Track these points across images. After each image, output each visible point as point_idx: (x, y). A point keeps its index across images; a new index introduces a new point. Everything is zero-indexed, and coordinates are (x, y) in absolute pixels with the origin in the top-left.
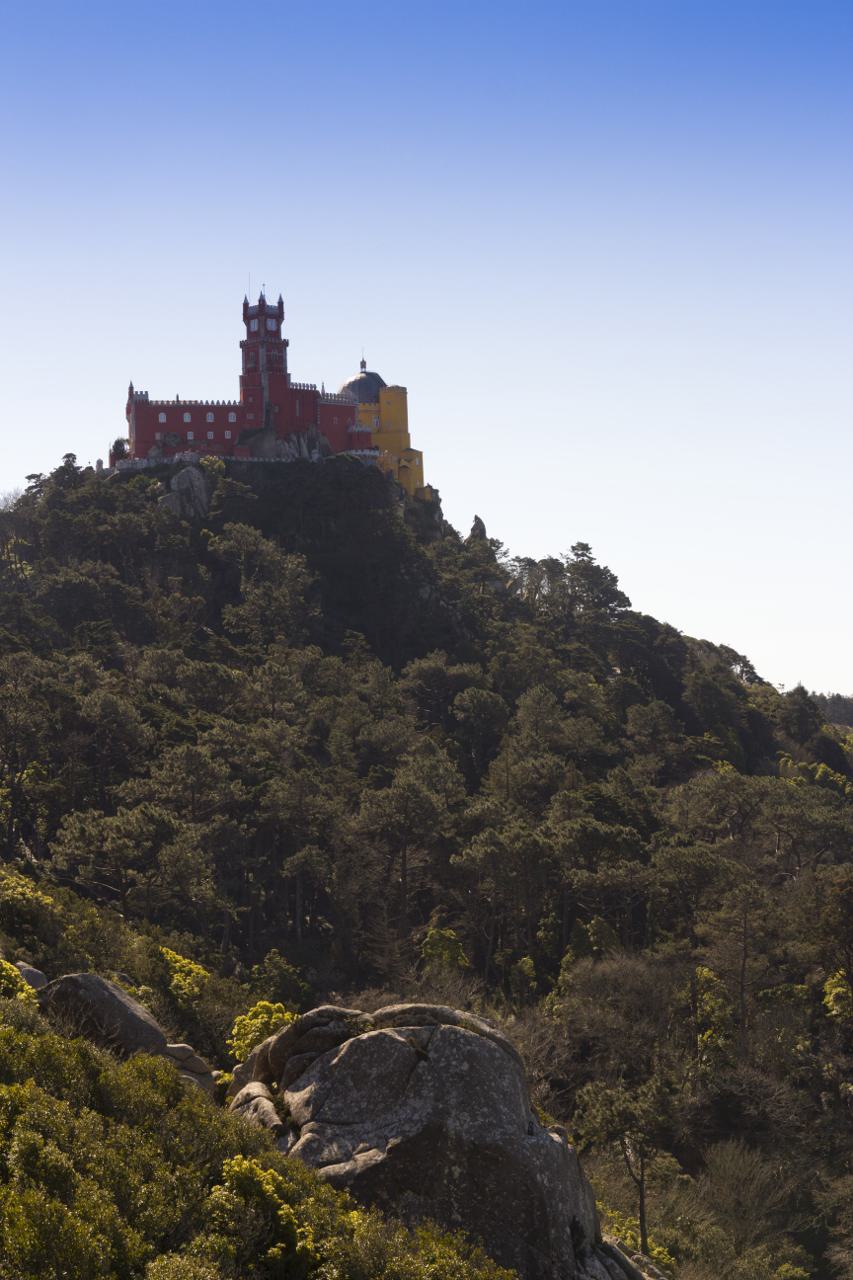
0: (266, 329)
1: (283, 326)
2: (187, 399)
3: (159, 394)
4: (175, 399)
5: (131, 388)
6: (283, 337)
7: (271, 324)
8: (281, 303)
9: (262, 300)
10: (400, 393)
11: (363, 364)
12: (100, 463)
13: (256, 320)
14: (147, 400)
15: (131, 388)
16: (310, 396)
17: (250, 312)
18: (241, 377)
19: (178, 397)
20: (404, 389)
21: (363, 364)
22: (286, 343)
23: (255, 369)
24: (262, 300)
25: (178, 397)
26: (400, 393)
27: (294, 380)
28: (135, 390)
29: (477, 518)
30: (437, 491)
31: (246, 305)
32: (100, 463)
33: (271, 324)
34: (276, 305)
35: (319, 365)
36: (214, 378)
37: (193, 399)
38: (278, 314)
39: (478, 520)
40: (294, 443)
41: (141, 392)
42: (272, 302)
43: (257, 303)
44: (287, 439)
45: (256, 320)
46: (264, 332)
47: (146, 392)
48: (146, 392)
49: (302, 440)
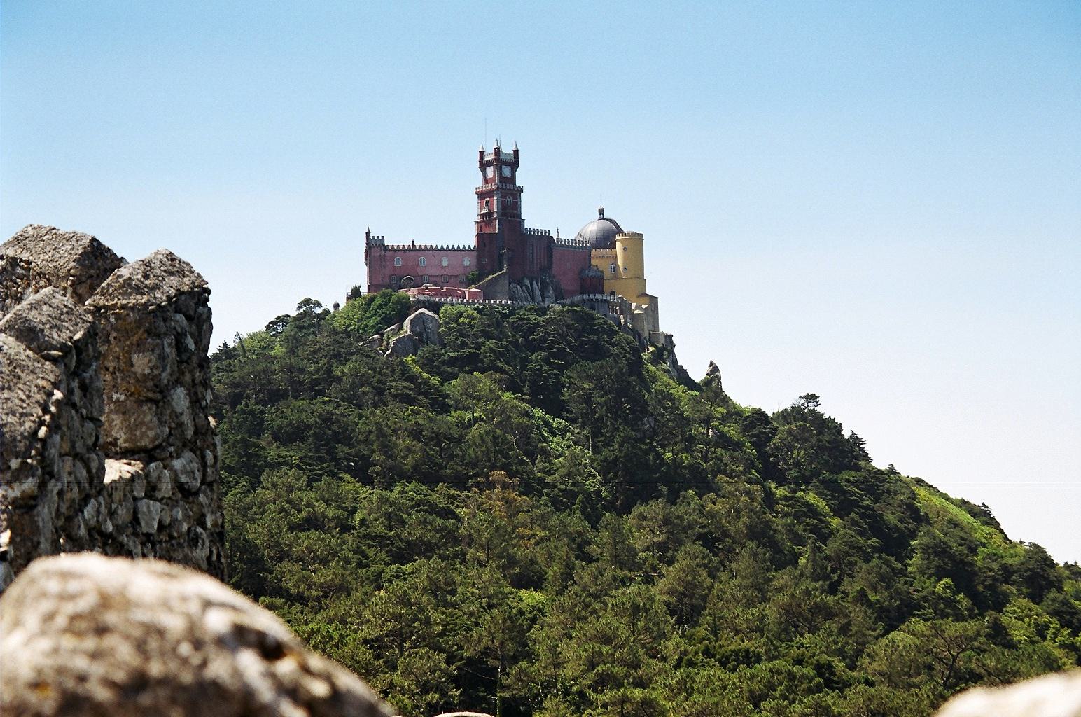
1: (518, 173)
2: (423, 244)
5: (368, 234)
6: (517, 185)
7: (507, 171)
8: (516, 152)
9: (498, 151)
10: (639, 237)
11: (601, 212)
12: (337, 306)
14: (383, 244)
15: (368, 234)
16: (546, 241)
17: (486, 159)
20: (642, 235)
21: (601, 212)
22: (521, 190)
23: (490, 214)
24: (498, 151)
26: (639, 237)
27: (527, 226)
29: (712, 364)
30: (671, 336)
31: (482, 153)
32: (337, 306)
34: (512, 152)
35: (554, 212)
36: (452, 224)
37: (428, 244)
38: (514, 163)
39: (712, 364)
40: (527, 288)
41: (378, 237)
42: (507, 150)
44: (520, 283)
45: (492, 167)
46: (502, 178)
47: (383, 237)
48: (383, 237)
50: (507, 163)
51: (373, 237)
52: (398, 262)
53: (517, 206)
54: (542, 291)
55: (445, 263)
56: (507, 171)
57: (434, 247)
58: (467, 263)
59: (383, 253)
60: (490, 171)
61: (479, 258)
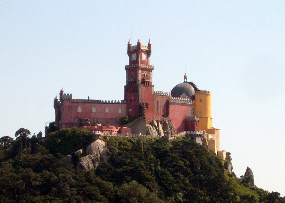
0: (141, 59)
1: (151, 57)
3: (78, 95)
4: (87, 99)
11: (185, 78)
13: (135, 54)
14: (71, 99)
17: (132, 49)
18: (125, 87)
19: (89, 97)
21: (185, 78)
25: (89, 97)
28: (63, 94)
33: (144, 56)
34: (148, 45)
41: (68, 94)
43: (136, 44)
45: (135, 54)
47: (71, 94)
48: (71, 94)
49: (160, 124)
50: (144, 51)
51: (65, 94)
52: (79, 110)
53: (149, 78)
54: (163, 128)
55: (107, 111)
56: (144, 56)
57: (101, 101)
58: (120, 111)
59: (71, 104)
60: (134, 57)
61: (128, 109)
